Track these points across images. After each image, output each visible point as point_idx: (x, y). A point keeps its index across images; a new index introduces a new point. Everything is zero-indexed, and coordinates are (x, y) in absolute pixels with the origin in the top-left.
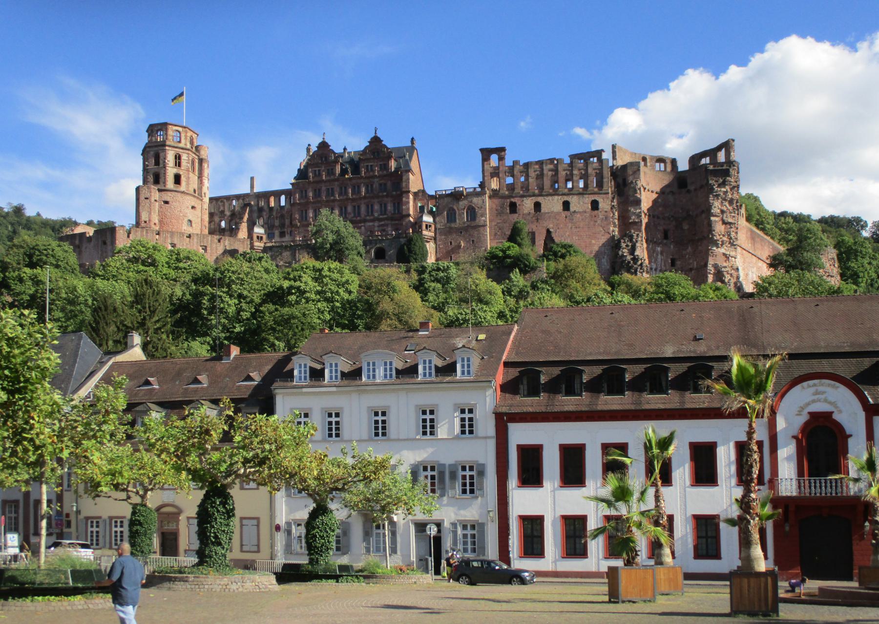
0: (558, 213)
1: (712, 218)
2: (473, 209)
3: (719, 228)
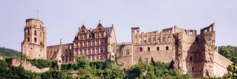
1: (205, 52)
3: (207, 57)
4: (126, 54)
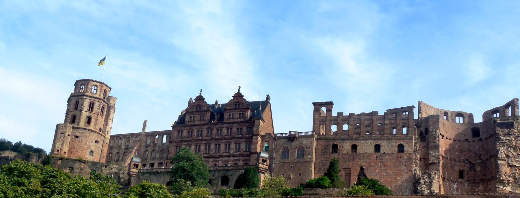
0: (371, 154)
1: (499, 162)
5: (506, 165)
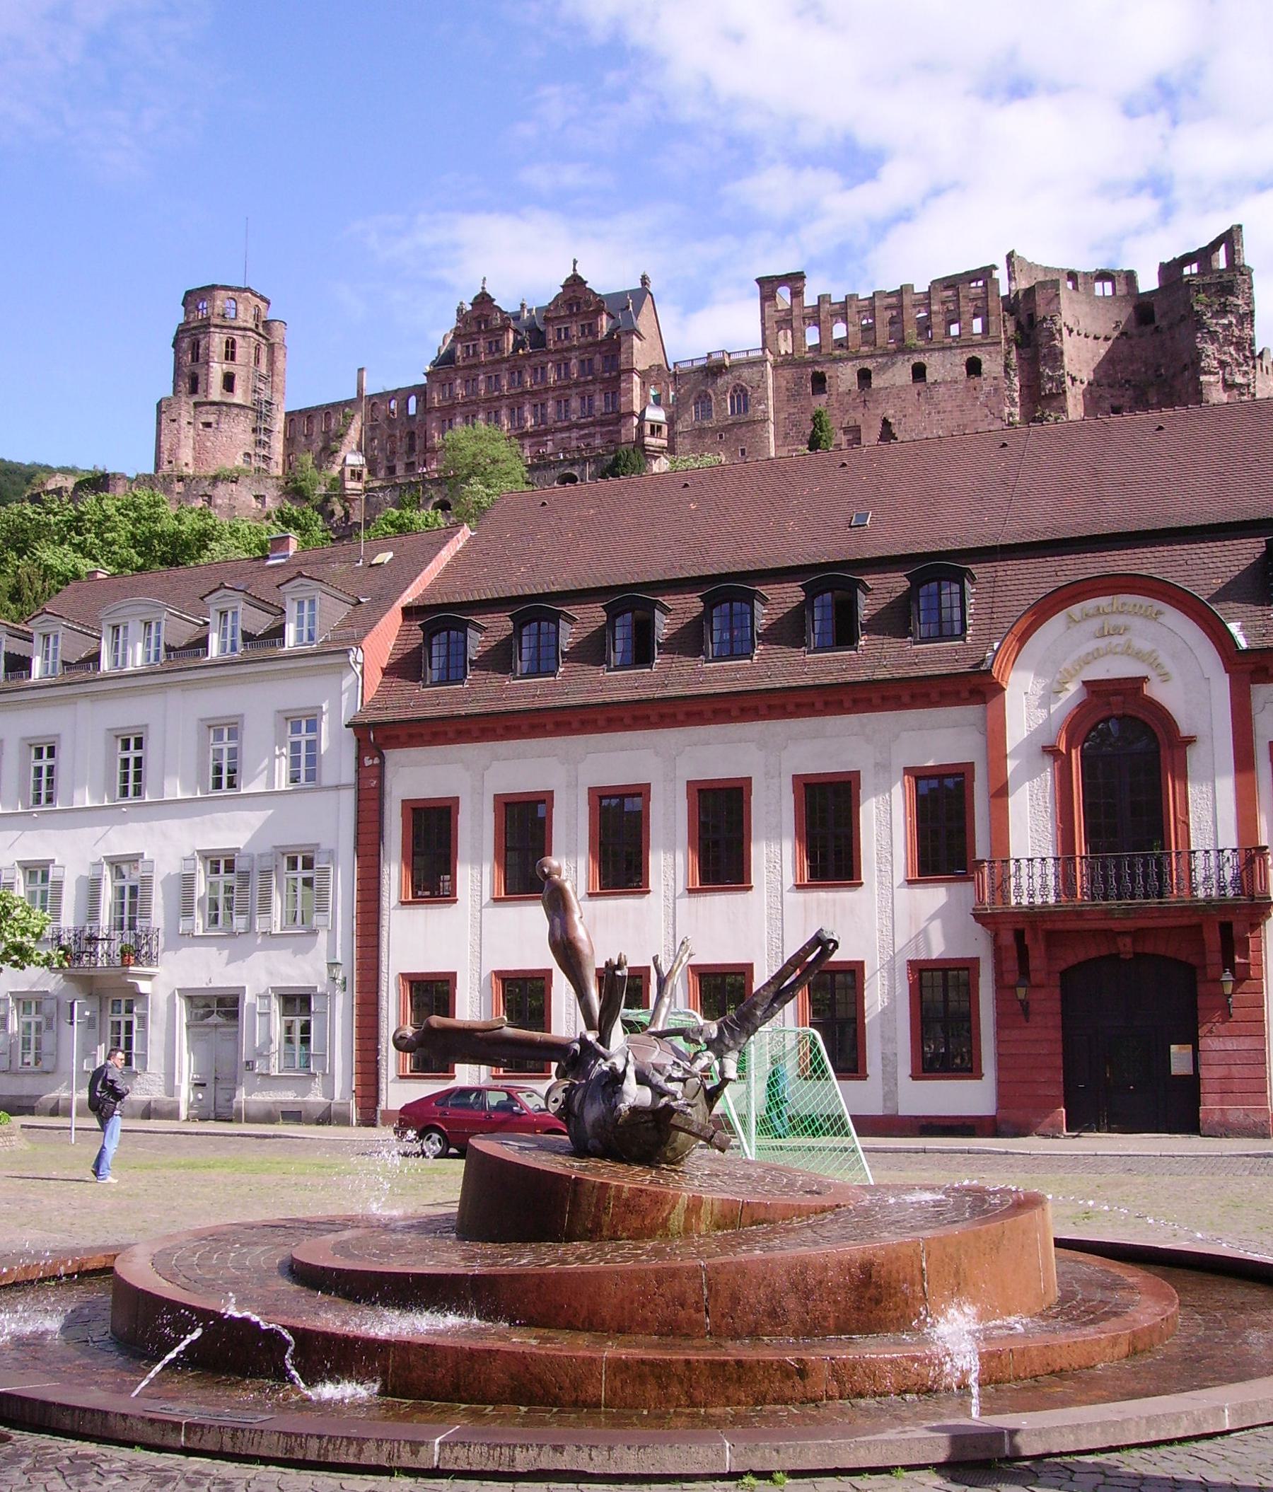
0: (903, 388)
1: (1203, 378)
2: (743, 390)
4: (733, 412)
5: (1220, 384)
